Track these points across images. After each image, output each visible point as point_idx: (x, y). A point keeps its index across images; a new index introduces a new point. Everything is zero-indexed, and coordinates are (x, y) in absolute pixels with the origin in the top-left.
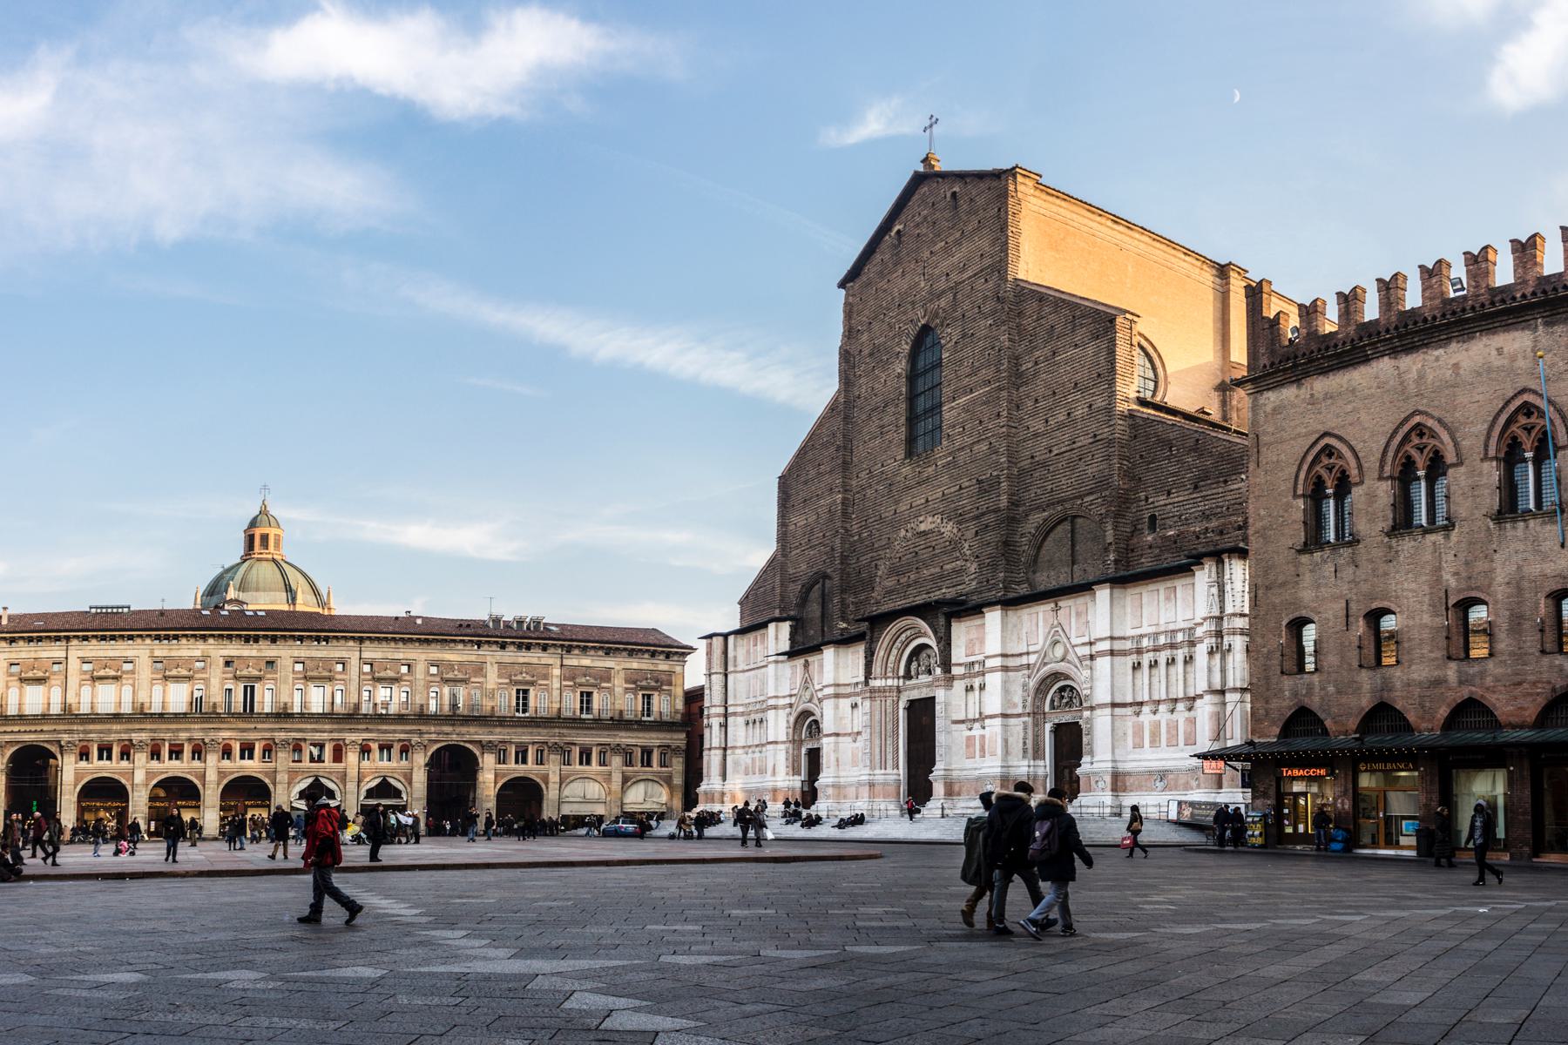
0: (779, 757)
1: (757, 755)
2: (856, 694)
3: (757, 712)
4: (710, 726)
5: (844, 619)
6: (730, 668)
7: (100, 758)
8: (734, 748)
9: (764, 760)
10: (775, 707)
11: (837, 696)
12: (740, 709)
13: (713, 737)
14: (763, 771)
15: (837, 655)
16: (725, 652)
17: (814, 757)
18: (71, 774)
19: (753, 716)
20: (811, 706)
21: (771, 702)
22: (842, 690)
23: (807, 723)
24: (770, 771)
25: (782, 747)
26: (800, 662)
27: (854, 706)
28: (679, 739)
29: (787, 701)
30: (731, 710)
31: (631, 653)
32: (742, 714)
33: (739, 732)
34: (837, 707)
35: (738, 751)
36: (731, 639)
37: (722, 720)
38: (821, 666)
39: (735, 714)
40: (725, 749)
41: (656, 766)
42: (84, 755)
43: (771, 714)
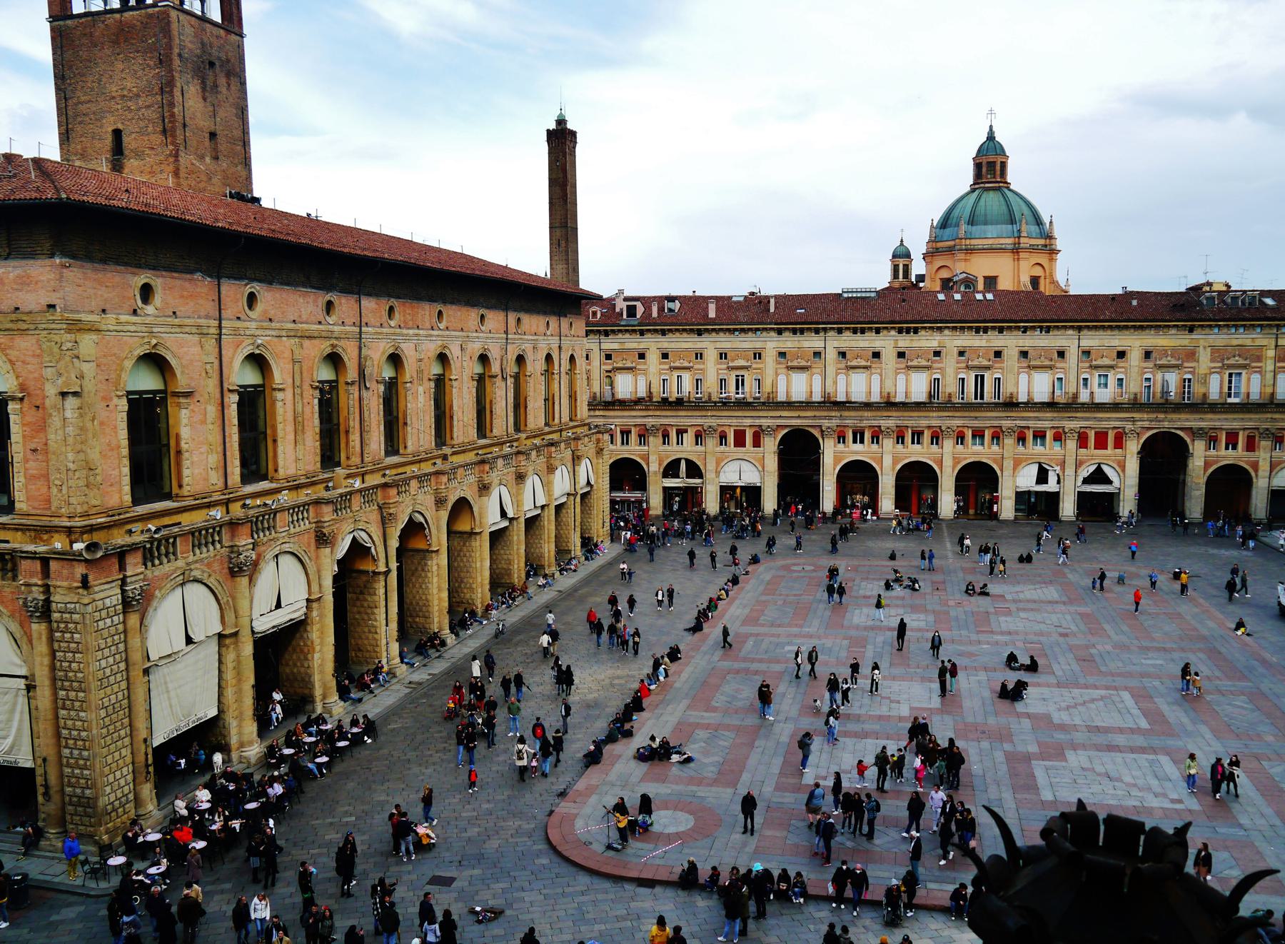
7: (855, 442)
18: (832, 457)
42: (841, 438)
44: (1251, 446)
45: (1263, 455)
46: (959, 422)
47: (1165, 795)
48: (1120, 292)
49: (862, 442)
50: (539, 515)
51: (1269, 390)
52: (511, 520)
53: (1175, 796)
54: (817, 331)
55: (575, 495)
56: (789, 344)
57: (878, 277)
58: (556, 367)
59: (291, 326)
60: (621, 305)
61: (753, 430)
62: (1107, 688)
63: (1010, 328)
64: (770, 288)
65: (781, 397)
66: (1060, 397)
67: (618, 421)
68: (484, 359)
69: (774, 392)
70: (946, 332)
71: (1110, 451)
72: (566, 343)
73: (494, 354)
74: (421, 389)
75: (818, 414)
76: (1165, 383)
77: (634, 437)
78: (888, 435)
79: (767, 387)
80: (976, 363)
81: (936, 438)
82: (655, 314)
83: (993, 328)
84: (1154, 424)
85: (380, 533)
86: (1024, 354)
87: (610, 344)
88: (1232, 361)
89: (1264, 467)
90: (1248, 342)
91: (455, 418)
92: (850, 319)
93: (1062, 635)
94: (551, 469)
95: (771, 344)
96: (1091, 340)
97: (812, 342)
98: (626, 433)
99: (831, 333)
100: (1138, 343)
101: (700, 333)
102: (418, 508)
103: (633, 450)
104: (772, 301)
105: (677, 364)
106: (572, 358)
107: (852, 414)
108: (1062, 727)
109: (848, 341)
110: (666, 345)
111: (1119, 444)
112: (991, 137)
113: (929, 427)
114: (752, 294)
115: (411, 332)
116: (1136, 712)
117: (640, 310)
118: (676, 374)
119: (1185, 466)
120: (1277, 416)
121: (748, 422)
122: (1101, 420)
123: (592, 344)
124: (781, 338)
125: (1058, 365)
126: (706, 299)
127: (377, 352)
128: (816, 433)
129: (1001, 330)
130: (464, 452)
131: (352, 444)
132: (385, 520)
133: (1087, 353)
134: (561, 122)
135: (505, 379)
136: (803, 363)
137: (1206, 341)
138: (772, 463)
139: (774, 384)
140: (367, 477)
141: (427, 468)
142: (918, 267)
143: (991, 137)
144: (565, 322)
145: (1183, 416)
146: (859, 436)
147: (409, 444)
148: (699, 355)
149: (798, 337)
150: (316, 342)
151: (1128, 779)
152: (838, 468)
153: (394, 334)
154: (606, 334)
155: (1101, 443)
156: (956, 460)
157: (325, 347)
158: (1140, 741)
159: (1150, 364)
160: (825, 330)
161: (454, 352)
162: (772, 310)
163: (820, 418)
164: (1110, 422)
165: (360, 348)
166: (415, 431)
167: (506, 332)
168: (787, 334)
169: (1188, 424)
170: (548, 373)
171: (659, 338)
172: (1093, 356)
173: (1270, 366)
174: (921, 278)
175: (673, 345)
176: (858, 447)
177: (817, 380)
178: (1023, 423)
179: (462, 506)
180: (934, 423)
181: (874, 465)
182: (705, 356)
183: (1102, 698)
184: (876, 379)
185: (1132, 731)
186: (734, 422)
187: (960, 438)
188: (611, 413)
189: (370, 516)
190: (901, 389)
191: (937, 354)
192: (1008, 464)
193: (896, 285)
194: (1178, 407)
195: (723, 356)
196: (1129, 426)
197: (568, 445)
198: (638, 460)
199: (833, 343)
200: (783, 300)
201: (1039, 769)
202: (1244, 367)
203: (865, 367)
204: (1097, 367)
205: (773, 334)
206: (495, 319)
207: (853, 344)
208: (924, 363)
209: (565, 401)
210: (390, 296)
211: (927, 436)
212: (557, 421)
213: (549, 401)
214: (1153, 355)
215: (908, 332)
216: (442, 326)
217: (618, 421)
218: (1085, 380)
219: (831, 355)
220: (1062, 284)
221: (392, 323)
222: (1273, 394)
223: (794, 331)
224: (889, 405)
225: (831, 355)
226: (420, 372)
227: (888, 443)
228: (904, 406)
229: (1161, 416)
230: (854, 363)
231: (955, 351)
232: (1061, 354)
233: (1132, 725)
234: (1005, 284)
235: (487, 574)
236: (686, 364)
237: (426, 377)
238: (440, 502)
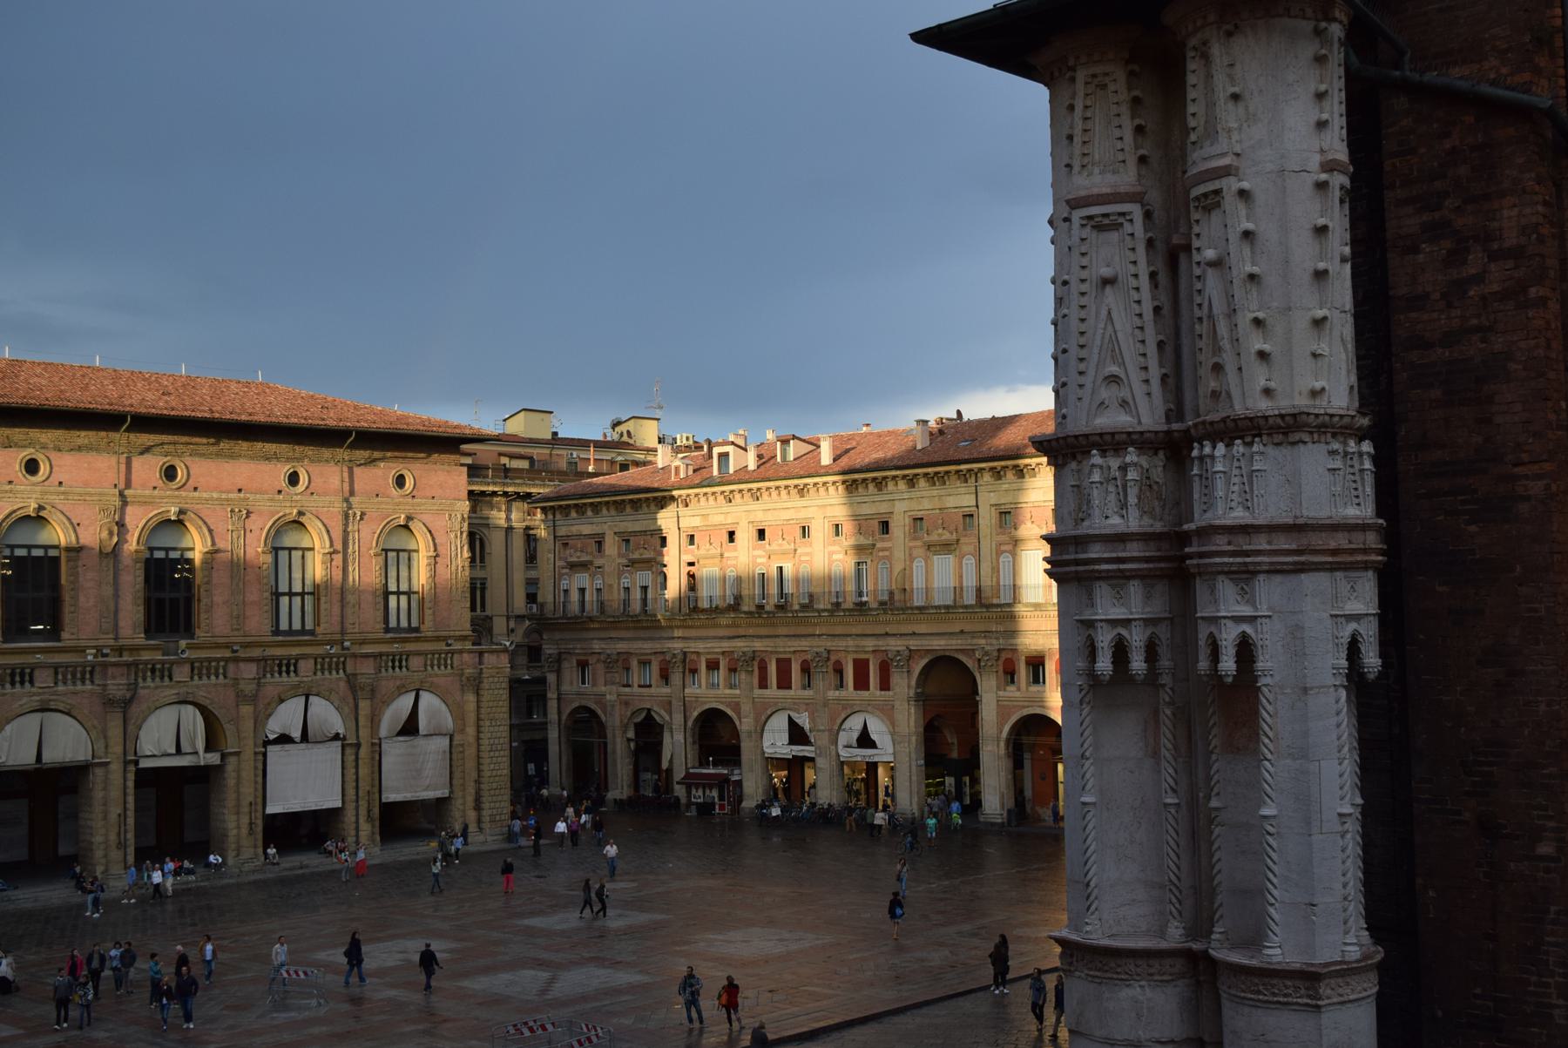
54: (963, 477)
56: (926, 504)
65: (918, 601)
67: (700, 646)
110: (760, 516)
121: (870, 644)
124: (915, 493)
128: (970, 663)
136: (947, 536)
138: (909, 719)
139: (906, 573)
152: (1007, 729)
163: (973, 634)
177: (969, 562)
186: (850, 642)
217: (700, 646)
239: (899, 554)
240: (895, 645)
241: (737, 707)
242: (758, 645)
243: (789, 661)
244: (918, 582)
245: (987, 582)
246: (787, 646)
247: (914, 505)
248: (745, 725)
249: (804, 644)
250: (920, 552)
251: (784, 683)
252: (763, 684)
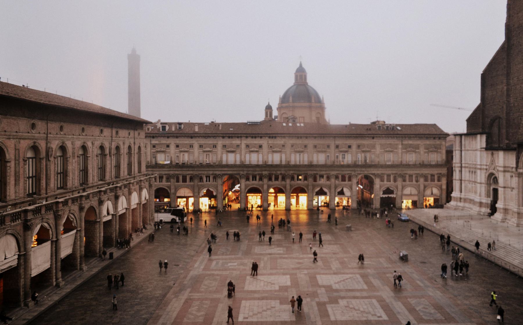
0: (482, 189)
1: (474, 185)
2: (512, 172)
3: (473, 168)
4: (455, 170)
5: (507, 139)
6: (463, 149)
7: (253, 180)
8: (465, 181)
9: (476, 188)
10: (481, 169)
11: (504, 171)
12: (467, 165)
13: (456, 175)
14: (476, 193)
15: (504, 154)
16: (461, 142)
17: (496, 191)
19: (471, 170)
20: (494, 172)
21: (479, 167)
22: (507, 169)
23: (492, 179)
24: (478, 194)
25: (483, 185)
26: (490, 152)
27: (512, 176)
28: (444, 171)
29: (485, 167)
30: (463, 165)
31: (427, 138)
32: (467, 167)
33: (466, 175)
34: (504, 176)
35: (467, 182)
36: (463, 137)
37: (460, 169)
38: (498, 156)
39: (465, 167)
40: (461, 180)
41: (436, 182)
42: (248, 179)
43: (478, 172)
44: (395, 181)
45: (399, 183)
46: (291, 172)
47: (375, 315)
48: (348, 124)
49: (256, 180)
50: (124, 214)
51: (400, 160)
52: (113, 215)
53: (379, 315)
54: (238, 137)
55: (140, 204)
56: (227, 142)
57: (259, 117)
58: (133, 151)
59: (15, 134)
60: (159, 126)
61: (213, 176)
62: (352, 273)
63: (309, 137)
64: (220, 120)
65: (224, 163)
66: (329, 163)
68: (102, 148)
69: (221, 161)
70: (287, 138)
71: (346, 182)
72: (137, 142)
73: (107, 145)
74: (74, 161)
75: (238, 169)
76: (366, 157)
77: (164, 179)
78: (265, 177)
79: (219, 159)
80: (298, 150)
81: (284, 179)
82: (173, 129)
83: (304, 137)
84: (362, 172)
85: (54, 223)
86: (315, 147)
87: (154, 141)
88: (387, 149)
89: (400, 187)
90: (392, 143)
91: (89, 172)
92: (250, 133)
93: (334, 254)
94: (130, 193)
95: (220, 142)
96: (339, 142)
97: (236, 141)
98: (161, 178)
99: (243, 138)
100: (355, 143)
101: (192, 137)
102: (72, 211)
103: (164, 184)
104: (220, 125)
105: (182, 150)
106: (139, 148)
107: (251, 169)
108: (337, 291)
109: (249, 141)
110: (178, 142)
111: (350, 180)
112: (301, 65)
113: (281, 174)
114: (212, 122)
115: (70, 136)
116: (362, 282)
117: (167, 128)
118: (182, 154)
119: (373, 188)
120: (403, 169)
122: (343, 171)
123: (147, 141)
125: (328, 150)
126: (194, 124)
127: (55, 145)
128: (238, 177)
129: (306, 137)
130: (93, 187)
131: (42, 185)
132: (57, 218)
133: (337, 147)
134: (134, 51)
135: (110, 156)
136: (233, 150)
137: (378, 142)
139: (221, 158)
140: (49, 199)
141: (76, 195)
142: (275, 113)
143: (301, 65)
144: (136, 133)
145: (372, 169)
146: (254, 178)
147: (68, 184)
148: (191, 146)
149: (230, 140)
150: (27, 141)
151: (362, 309)
153: (63, 137)
154: (153, 137)
155: (343, 180)
156: (291, 186)
157: (30, 143)
158: (365, 294)
159: (360, 150)
160: (241, 137)
161: (89, 144)
162: (220, 128)
163: (240, 171)
164: (347, 172)
165: (47, 144)
166: (71, 178)
167: (112, 137)
168: (226, 138)
169: (373, 172)
170: (130, 153)
171: (176, 140)
172: (340, 147)
173: (400, 151)
174: (276, 117)
175: (181, 142)
176: (254, 182)
177: (238, 156)
178: (315, 172)
179: (92, 209)
180: (283, 172)
181: (260, 189)
182: (194, 147)
183: (350, 278)
184: (261, 156)
185: (362, 290)
186: (206, 172)
187: (293, 178)
188: (155, 169)
189: (51, 216)
190: (270, 159)
191: (283, 146)
192: (310, 187)
193: (267, 120)
194: (370, 166)
195: (201, 146)
196: (353, 173)
197: (137, 183)
198: (166, 188)
199: (244, 142)
200: (225, 125)
201: (329, 308)
202: (392, 151)
203: (257, 151)
204: (341, 151)
205: (221, 138)
206: (107, 132)
207: (252, 142)
208: (278, 150)
209: (136, 165)
210: (61, 121)
211: (280, 177)
212: (133, 173)
213: (130, 165)
214: (361, 147)
215: (272, 137)
216: (84, 134)
218: (337, 156)
219: (243, 146)
220: (327, 120)
221: (62, 133)
222: (401, 161)
223: (229, 137)
224: (266, 166)
225: (243, 146)
226: (73, 153)
227: (265, 180)
228: (272, 166)
229: (364, 169)
230: (252, 150)
231: (290, 145)
232: (328, 146)
233: (361, 288)
234: (307, 120)
235: (102, 239)
236: (186, 150)
237: (76, 155)
238: (81, 209)
239: (219, 153)
240: (217, 173)
241: (169, 187)
242: (177, 172)
243: (186, 176)
244: (224, 159)
245: (243, 160)
246: (185, 173)
247: (224, 142)
248: (173, 191)
249: (191, 172)
250: (225, 152)
251: (184, 180)
252: (178, 181)
